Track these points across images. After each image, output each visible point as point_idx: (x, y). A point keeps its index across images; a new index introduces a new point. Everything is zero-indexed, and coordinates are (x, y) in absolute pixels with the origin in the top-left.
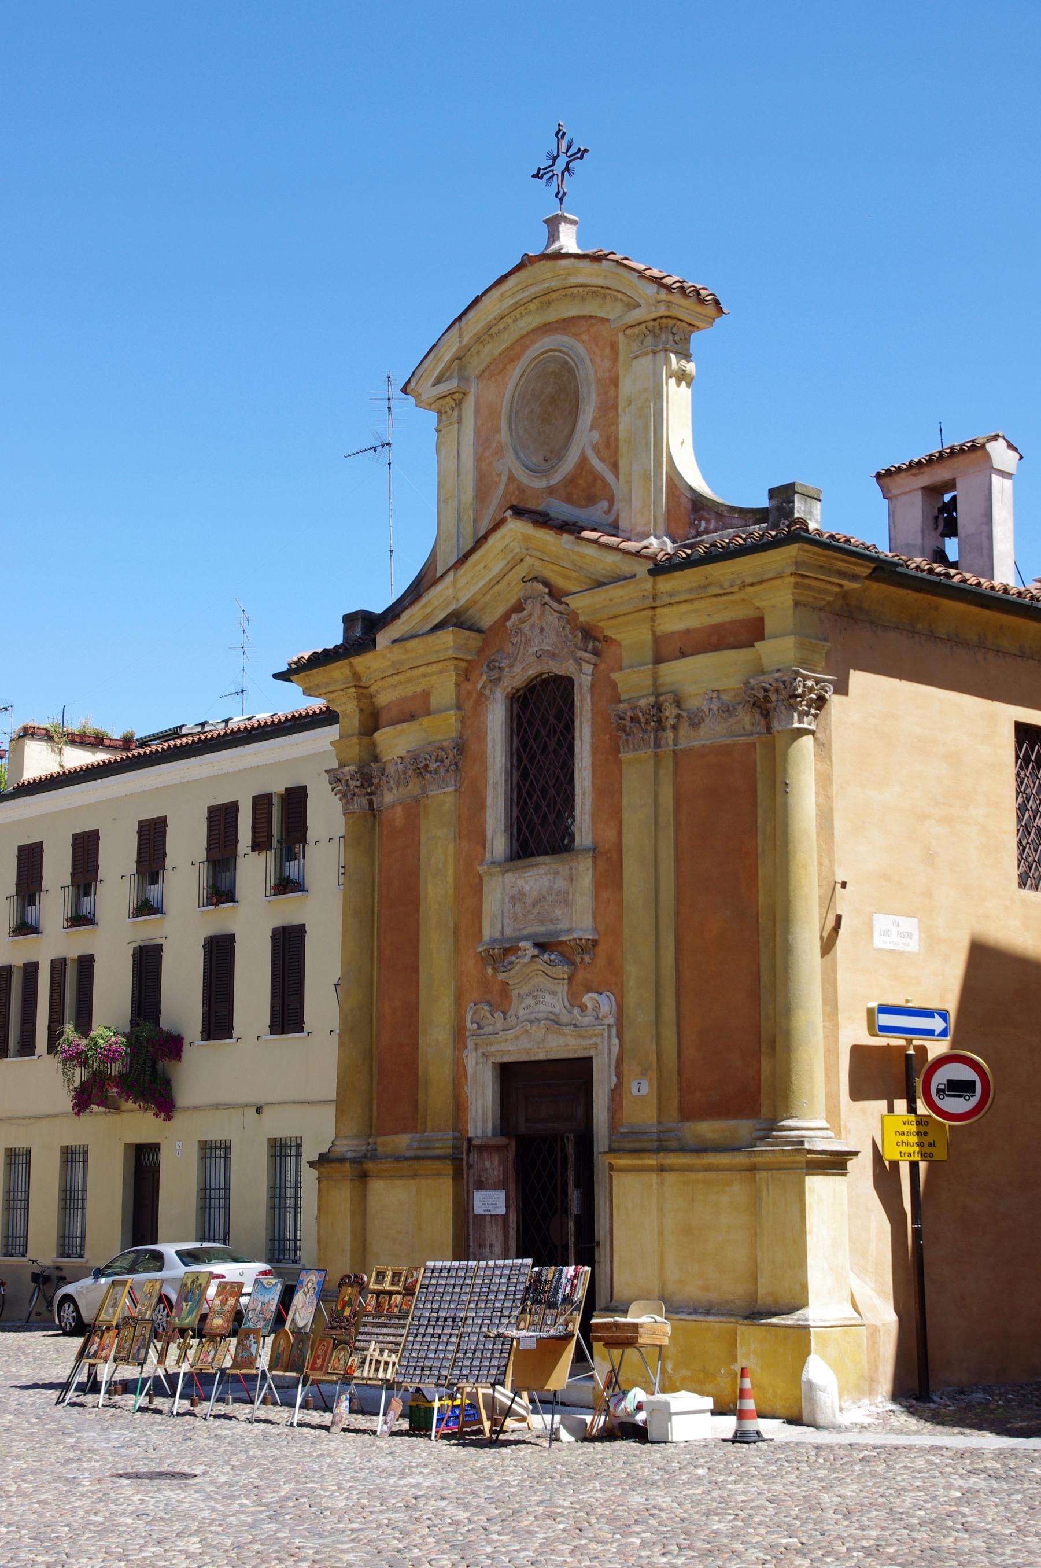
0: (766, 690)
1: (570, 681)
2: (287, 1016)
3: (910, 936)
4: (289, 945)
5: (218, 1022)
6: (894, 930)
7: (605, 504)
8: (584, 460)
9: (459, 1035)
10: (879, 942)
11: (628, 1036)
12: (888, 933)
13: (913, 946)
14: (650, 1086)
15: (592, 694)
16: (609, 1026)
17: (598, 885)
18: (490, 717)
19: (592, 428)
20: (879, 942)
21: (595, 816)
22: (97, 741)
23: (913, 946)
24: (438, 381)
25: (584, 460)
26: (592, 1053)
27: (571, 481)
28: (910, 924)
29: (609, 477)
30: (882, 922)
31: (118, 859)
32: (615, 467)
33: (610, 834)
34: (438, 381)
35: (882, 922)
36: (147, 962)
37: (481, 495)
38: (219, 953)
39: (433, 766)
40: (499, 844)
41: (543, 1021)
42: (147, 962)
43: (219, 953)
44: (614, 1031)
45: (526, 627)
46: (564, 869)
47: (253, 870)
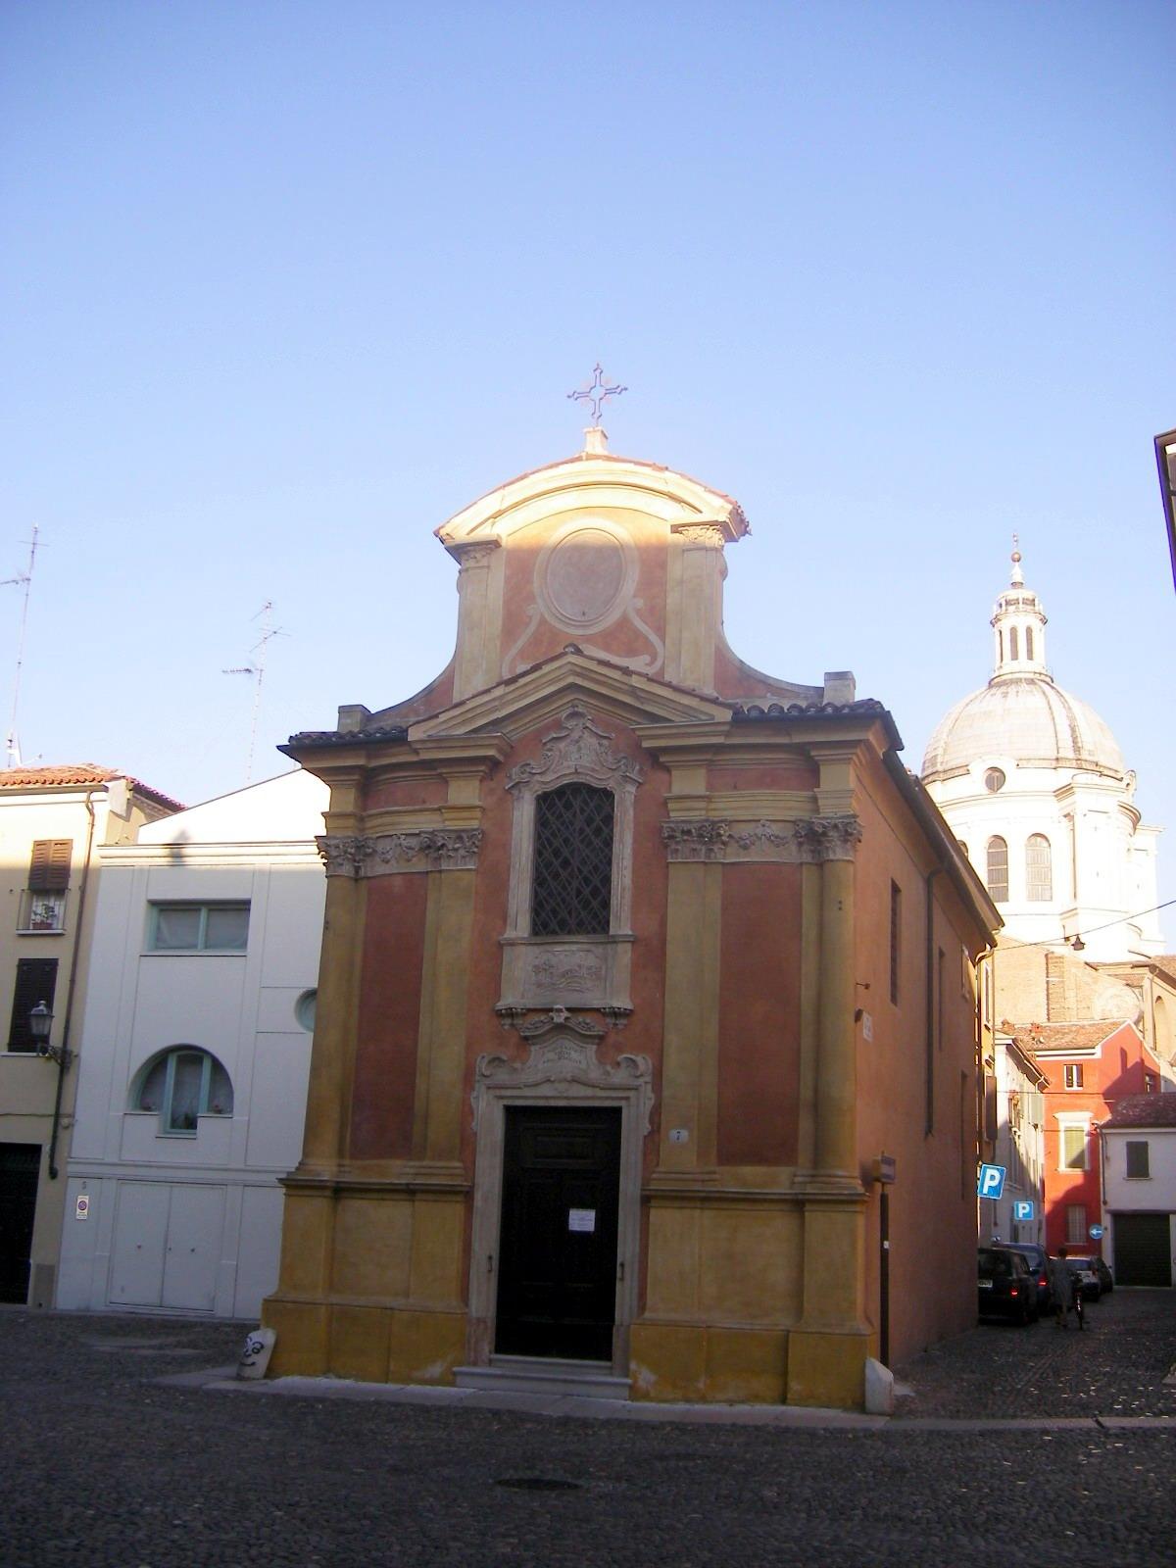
0: (824, 827)
1: (608, 795)
7: (647, 658)
9: (468, 1079)
11: (666, 1093)
15: (635, 809)
16: (646, 1083)
17: (636, 967)
18: (516, 813)
19: (635, 596)
21: (636, 907)
26: (623, 1103)
29: (654, 638)
32: (661, 632)
37: (510, 630)
40: (521, 924)
41: (562, 1074)
44: (649, 1087)
45: (562, 745)
46: (599, 950)
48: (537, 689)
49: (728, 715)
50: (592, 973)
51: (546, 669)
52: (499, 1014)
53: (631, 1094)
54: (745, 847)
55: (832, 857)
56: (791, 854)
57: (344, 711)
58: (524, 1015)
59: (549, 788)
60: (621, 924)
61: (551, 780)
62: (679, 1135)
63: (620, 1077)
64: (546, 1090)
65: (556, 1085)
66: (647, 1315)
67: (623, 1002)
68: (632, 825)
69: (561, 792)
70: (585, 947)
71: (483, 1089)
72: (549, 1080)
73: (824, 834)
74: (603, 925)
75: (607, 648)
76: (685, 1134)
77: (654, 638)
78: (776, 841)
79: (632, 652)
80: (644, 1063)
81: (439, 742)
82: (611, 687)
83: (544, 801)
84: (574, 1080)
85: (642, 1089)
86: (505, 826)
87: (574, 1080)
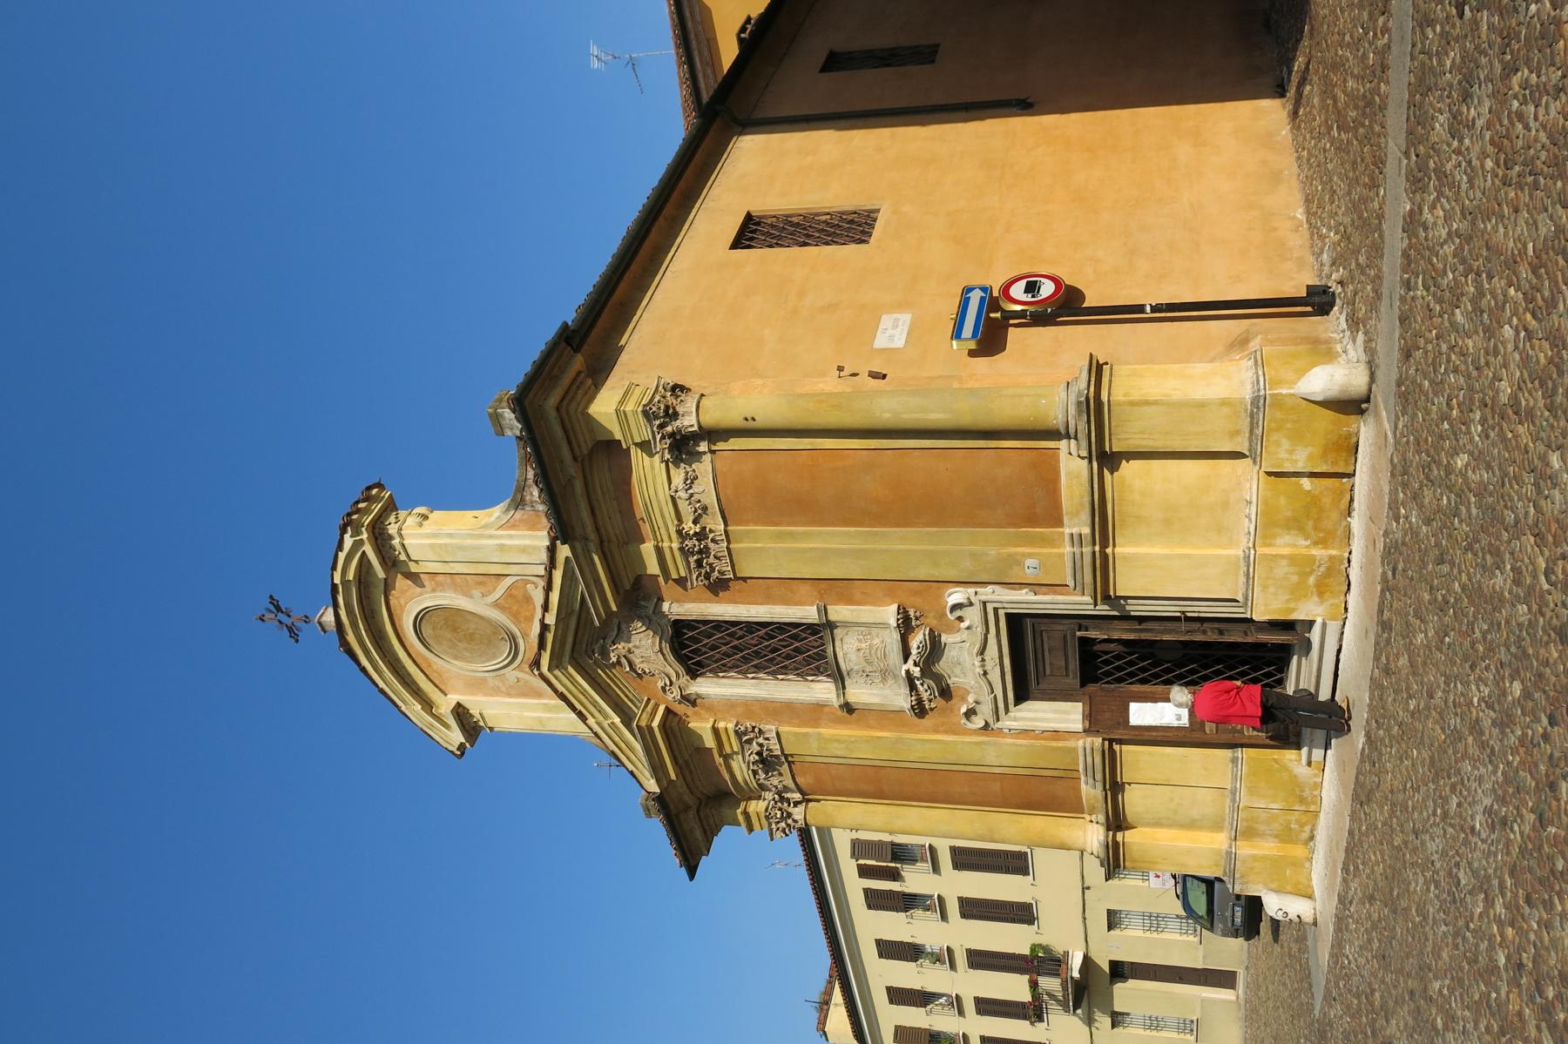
0: (663, 437)
2: (1016, 863)
3: (896, 320)
4: (966, 859)
5: (1022, 913)
6: (890, 332)
8: (496, 605)
10: (899, 343)
12: (891, 337)
13: (905, 318)
14: (1030, 555)
17: (850, 601)
20: (899, 343)
22: (830, 983)
23: (905, 318)
24: (447, 726)
25: (496, 605)
27: (515, 617)
28: (886, 320)
29: (508, 581)
30: (881, 342)
31: (906, 975)
33: (804, 589)
34: (447, 726)
35: (881, 342)
36: (981, 960)
37: (539, 695)
38: (974, 909)
39: (756, 748)
40: (822, 690)
42: (981, 960)
43: (974, 909)
45: (637, 661)
47: (915, 880)
48: (584, 693)
49: (564, 551)
50: (866, 633)
51: (561, 689)
52: (920, 710)
53: (990, 608)
54: (705, 509)
55: (696, 428)
56: (704, 467)
57: (649, 815)
58: (918, 694)
59: (681, 670)
60: (808, 613)
61: (672, 668)
62: (1030, 568)
63: (973, 616)
64: (995, 676)
65: (988, 668)
66: (1240, 598)
67: (890, 614)
68: (702, 606)
69: (682, 659)
70: (837, 643)
71: (999, 725)
72: (985, 673)
73: (672, 435)
74: (812, 629)
75: (530, 619)
76: (1029, 562)
77: (508, 581)
78: (690, 481)
79: (528, 599)
80: (956, 596)
81: (657, 770)
82: (563, 644)
83: (693, 674)
84: (982, 652)
85: (984, 598)
86: (730, 705)
87: (982, 652)
